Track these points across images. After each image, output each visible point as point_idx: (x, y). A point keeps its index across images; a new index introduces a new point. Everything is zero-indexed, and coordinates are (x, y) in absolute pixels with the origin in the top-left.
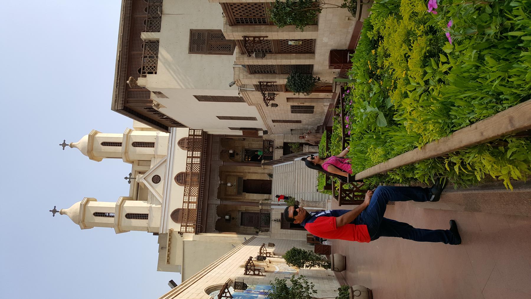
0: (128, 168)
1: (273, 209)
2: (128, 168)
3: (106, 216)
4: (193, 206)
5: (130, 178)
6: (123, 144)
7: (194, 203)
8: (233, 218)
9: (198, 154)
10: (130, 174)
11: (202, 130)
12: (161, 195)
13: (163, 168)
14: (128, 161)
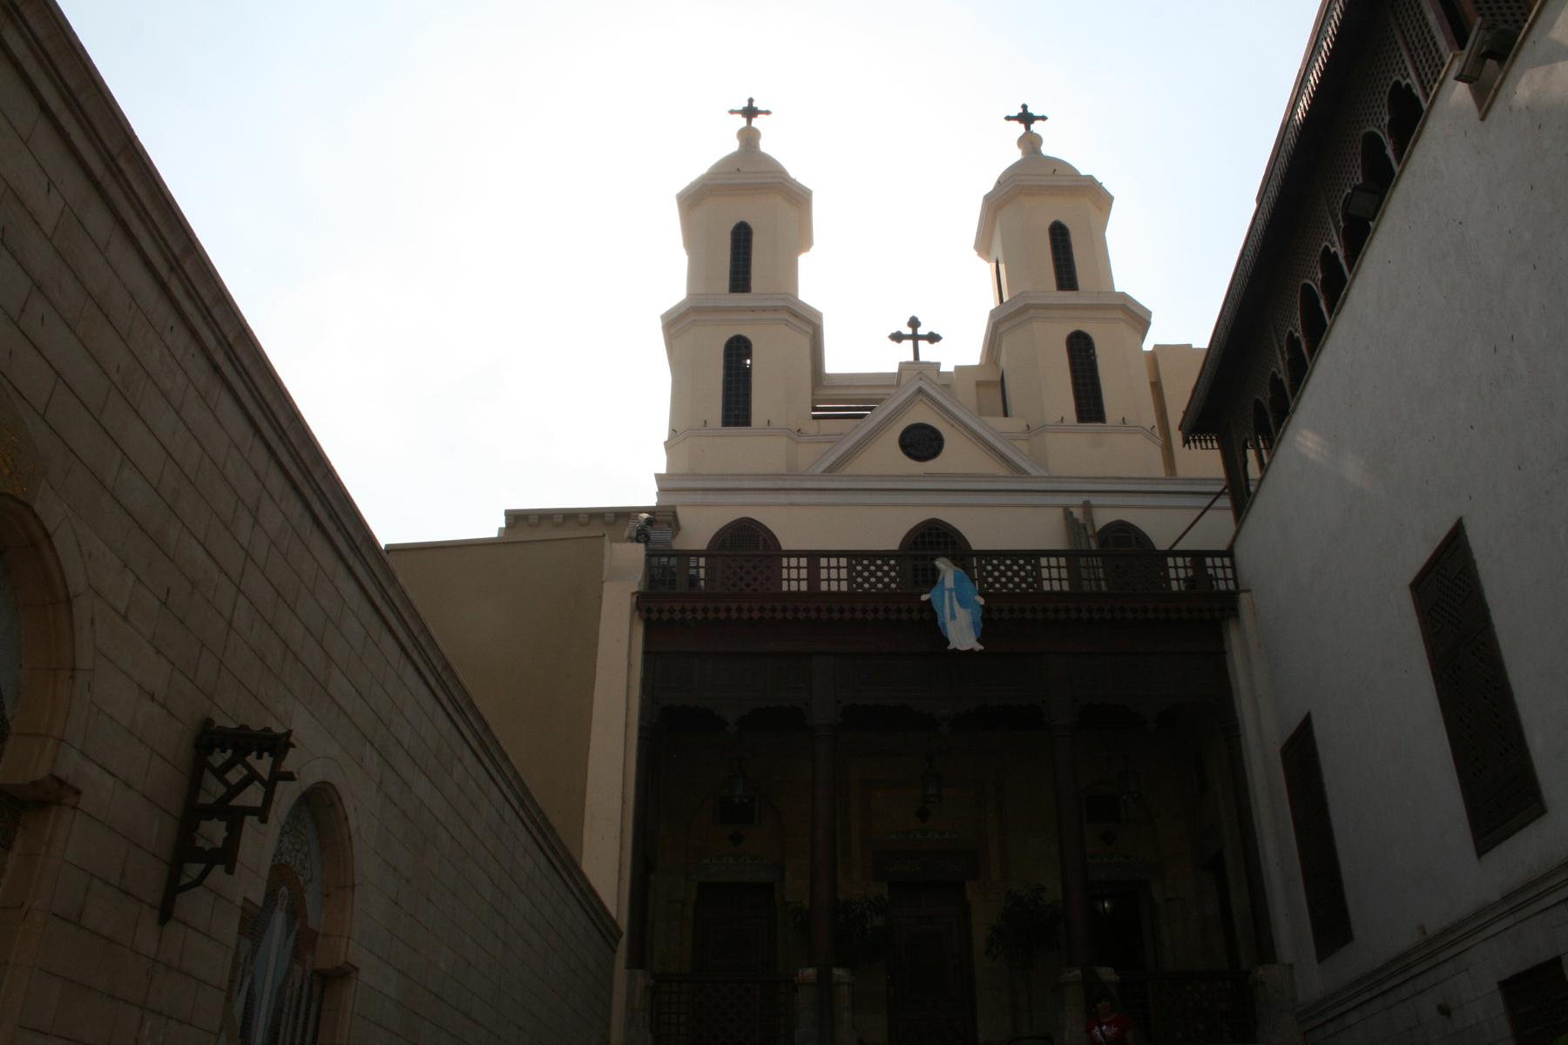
2: (961, 347)
5: (915, 338)
6: (1067, 297)
7: (813, 578)
10: (933, 338)
11: (1237, 591)
12: (851, 469)
13: (980, 463)
14: (1001, 325)
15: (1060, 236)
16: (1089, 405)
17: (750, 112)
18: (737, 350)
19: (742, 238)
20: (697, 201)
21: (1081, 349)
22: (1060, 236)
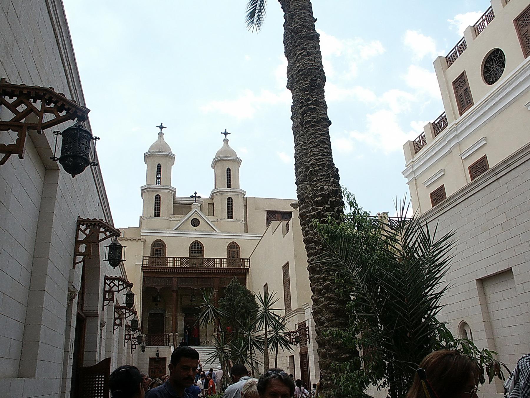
0: (205, 194)
1: (170, 348)
3: (157, 174)
4: (170, 264)
5: (196, 197)
8: (156, 305)
9: (225, 265)
10: (199, 197)
15: (229, 170)
16: (230, 216)
17: (161, 127)
18: (158, 198)
19: (159, 167)
20: (148, 157)
21: (230, 201)
22: (229, 170)
